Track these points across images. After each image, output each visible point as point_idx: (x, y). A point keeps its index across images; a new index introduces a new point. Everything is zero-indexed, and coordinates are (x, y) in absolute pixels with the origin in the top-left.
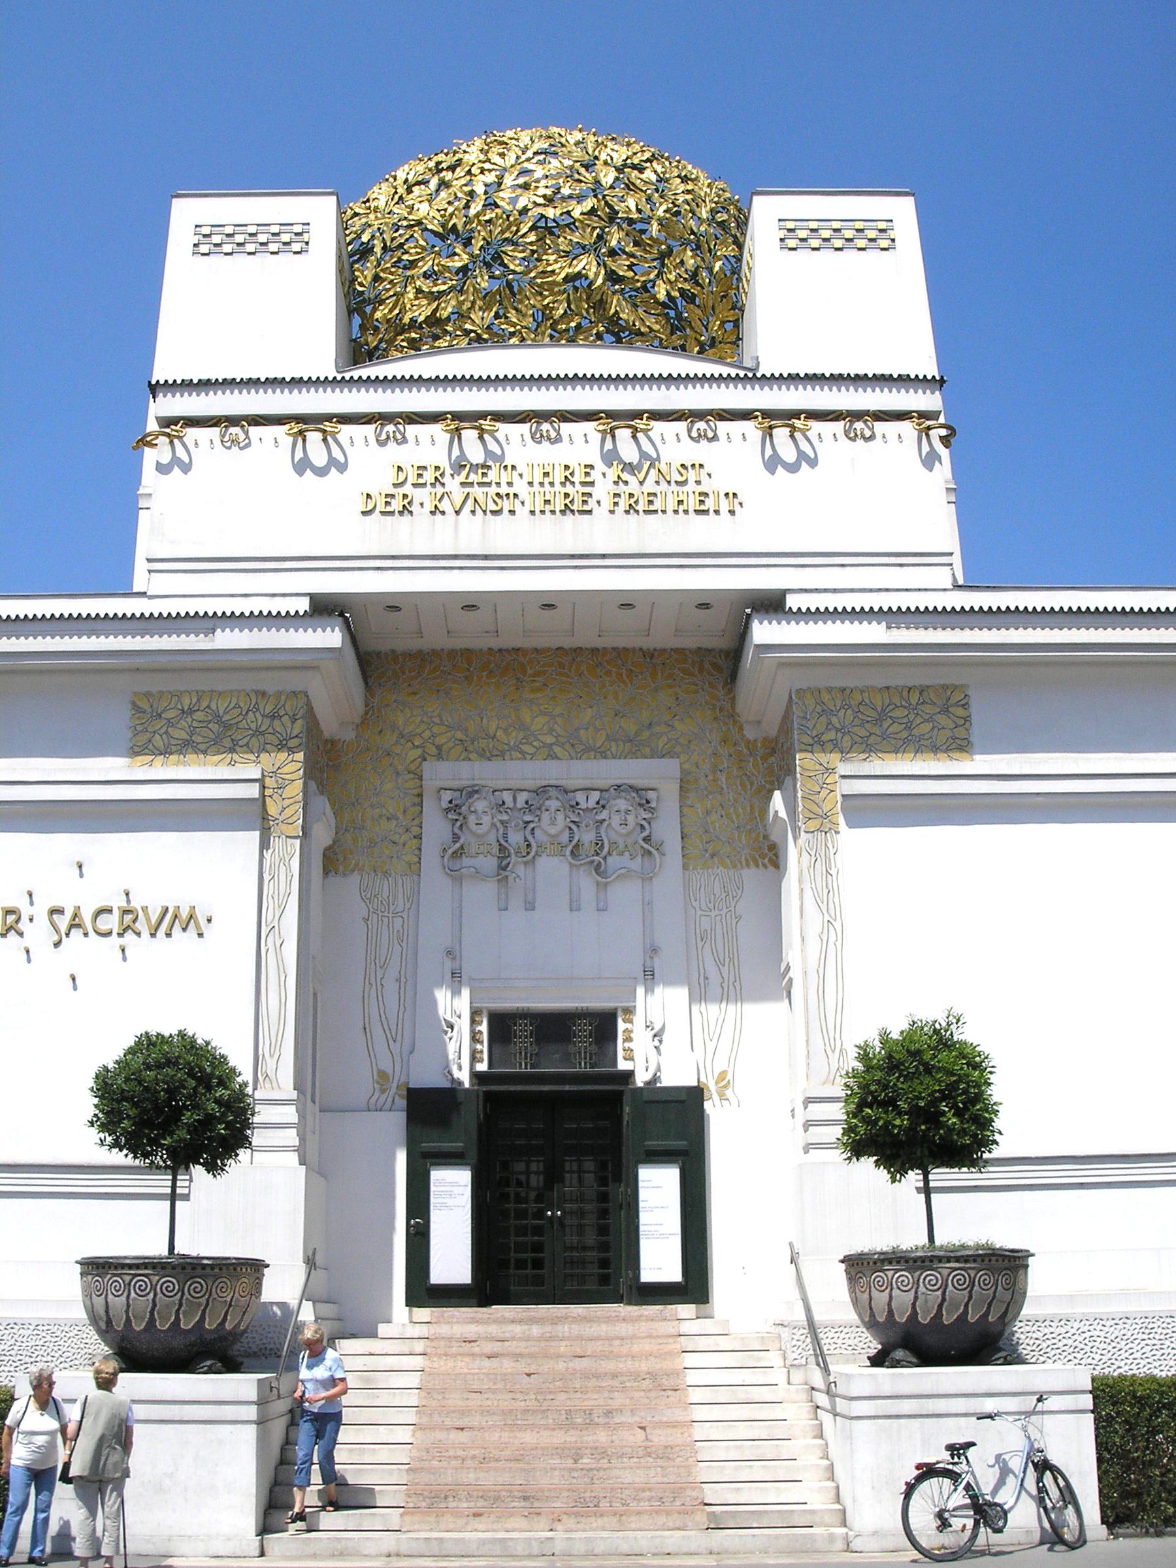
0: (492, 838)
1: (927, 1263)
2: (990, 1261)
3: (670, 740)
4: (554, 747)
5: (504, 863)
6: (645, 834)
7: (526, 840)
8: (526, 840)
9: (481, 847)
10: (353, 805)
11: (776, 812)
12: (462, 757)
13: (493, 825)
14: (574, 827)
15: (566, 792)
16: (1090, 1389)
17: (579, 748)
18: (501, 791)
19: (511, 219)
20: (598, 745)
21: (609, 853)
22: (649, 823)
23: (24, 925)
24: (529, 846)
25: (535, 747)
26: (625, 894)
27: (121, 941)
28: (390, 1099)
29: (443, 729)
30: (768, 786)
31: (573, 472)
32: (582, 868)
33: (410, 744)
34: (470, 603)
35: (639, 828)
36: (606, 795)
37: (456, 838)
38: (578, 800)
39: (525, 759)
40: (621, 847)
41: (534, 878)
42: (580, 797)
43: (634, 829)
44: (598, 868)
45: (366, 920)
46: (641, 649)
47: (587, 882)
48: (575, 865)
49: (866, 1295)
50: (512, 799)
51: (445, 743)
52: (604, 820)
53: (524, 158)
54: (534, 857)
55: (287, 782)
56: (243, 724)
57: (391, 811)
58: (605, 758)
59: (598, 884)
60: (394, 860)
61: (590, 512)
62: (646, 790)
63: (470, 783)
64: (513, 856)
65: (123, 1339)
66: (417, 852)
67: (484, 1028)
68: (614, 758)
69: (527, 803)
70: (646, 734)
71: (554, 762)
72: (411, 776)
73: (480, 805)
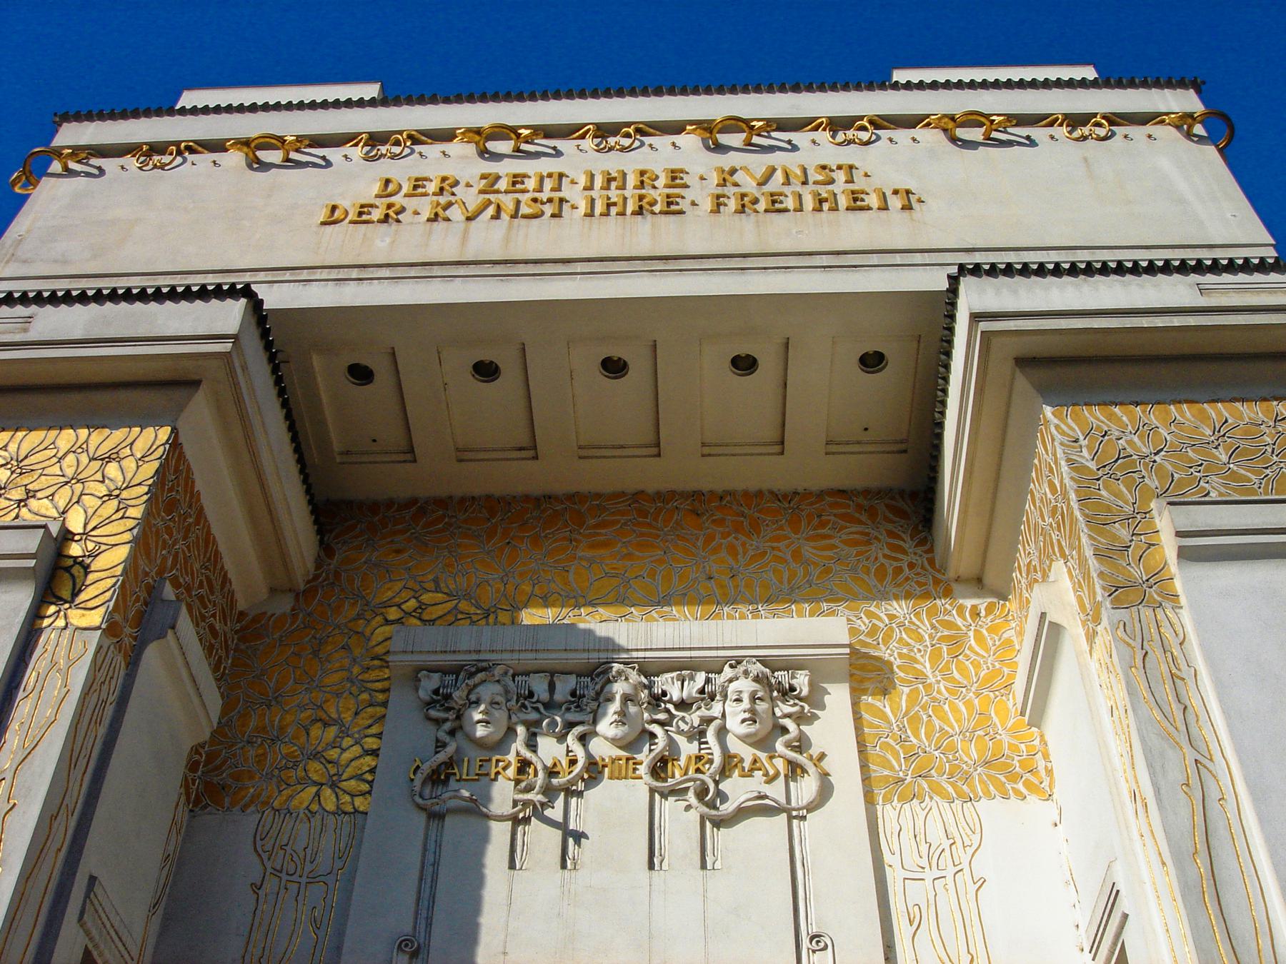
10: (269, 706)
14: (656, 729)
18: (527, 674)
21: (724, 772)
33: (379, 619)
38: (664, 687)
45: (256, 888)
46: (771, 492)
50: (546, 687)
52: (716, 718)
55: (103, 547)
56: (56, 470)
61: (681, 212)
62: (792, 666)
63: (475, 657)
66: (369, 778)
69: (573, 694)
72: (376, 662)
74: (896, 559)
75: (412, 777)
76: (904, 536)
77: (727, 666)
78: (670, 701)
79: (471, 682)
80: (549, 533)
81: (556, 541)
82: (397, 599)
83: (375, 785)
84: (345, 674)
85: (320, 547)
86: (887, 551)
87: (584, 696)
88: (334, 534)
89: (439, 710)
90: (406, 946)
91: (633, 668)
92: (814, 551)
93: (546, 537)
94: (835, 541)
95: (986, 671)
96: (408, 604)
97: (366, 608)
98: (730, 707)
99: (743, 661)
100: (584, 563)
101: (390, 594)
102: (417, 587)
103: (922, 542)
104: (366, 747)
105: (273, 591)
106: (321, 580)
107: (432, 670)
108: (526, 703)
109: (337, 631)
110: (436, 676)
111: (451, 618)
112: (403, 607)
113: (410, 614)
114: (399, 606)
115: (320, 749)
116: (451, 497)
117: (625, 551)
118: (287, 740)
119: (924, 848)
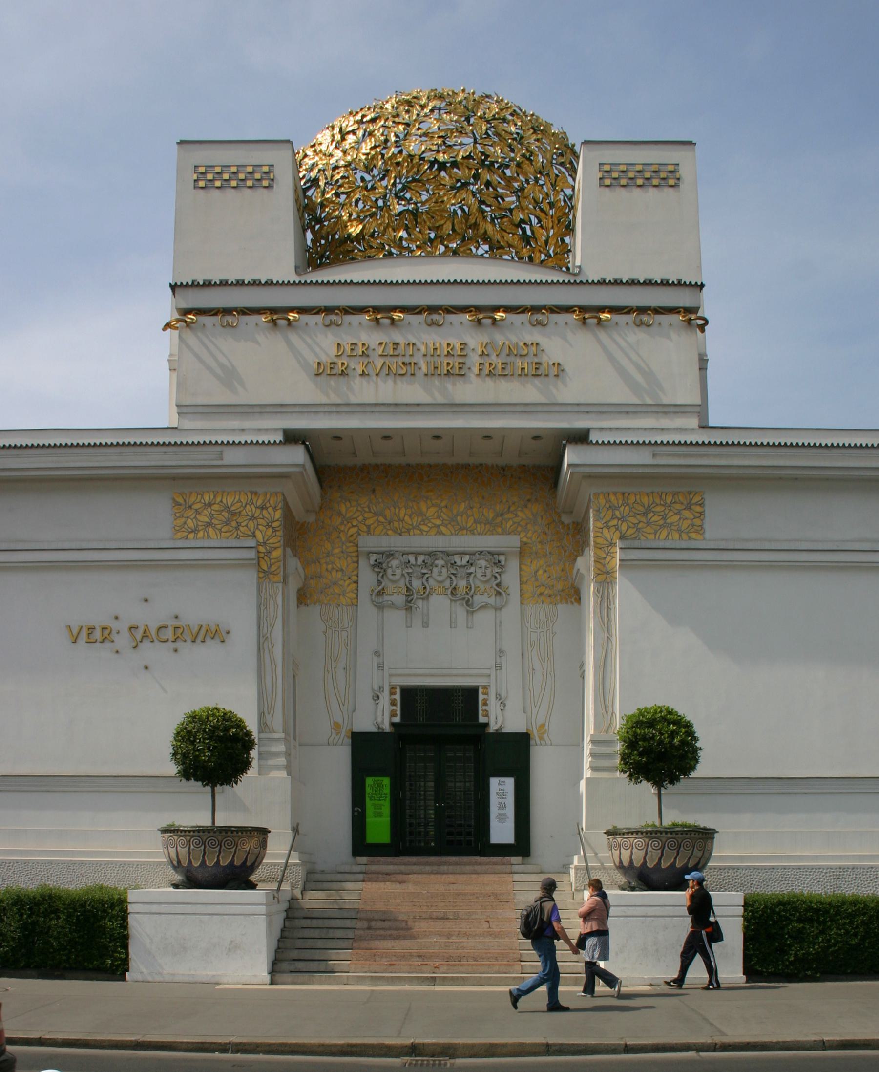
0: (402, 584)
1: (654, 835)
2: (691, 834)
3: (514, 523)
4: (441, 527)
5: (409, 599)
6: (498, 581)
7: (423, 584)
8: (423, 584)
9: (395, 589)
11: (579, 570)
12: (383, 533)
13: (403, 575)
14: (453, 577)
15: (448, 555)
16: (743, 904)
17: (457, 527)
18: (408, 554)
19: (414, 162)
20: (468, 526)
22: (500, 575)
23: (114, 636)
24: (425, 588)
25: (429, 527)
26: (484, 618)
27: (174, 645)
29: (371, 515)
30: (575, 553)
31: (453, 346)
32: (458, 603)
33: (350, 525)
34: (387, 436)
37: (379, 583)
39: (422, 534)
40: (483, 590)
41: (428, 610)
42: (457, 559)
43: (490, 579)
46: (497, 466)
47: (460, 611)
48: (454, 600)
49: (618, 851)
50: (414, 558)
51: (372, 524)
52: (472, 573)
53: (422, 114)
54: (428, 595)
57: (338, 565)
58: (473, 534)
59: (468, 611)
60: (341, 597)
62: (499, 554)
63: (388, 549)
64: (415, 595)
65: (188, 871)
66: (356, 592)
68: (479, 534)
69: (424, 561)
70: (500, 519)
71: (441, 536)
72: (351, 544)
73: (395, 563)
79: (388, 560)
98: (479, 570)
100: (425, 499)
101: (351, 514)
107: (375, 553)
111: (376, 525)
114: (356, 519)
117: (439, 493)
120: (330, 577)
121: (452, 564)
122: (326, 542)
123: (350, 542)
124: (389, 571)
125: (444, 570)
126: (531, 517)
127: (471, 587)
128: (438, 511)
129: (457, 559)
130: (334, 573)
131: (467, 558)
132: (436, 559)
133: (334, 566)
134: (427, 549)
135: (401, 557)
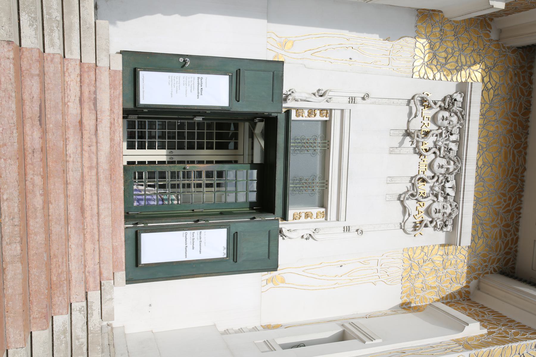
10: (454, 36)
28: (273, 48)
32: (410, 184)
33: (485, 74)
35: (430, 219)
36: (452, 200)
44: (412, 195)
46: (520, 217)
50: (455, 139)
52: (438, 199)
62: (454, 225)
66: (425, 77)
67: (318, 117)
69: (451, 149)
73: (455, 119)
74: (489, 262)
75: (425, 93)
76: (498, 264)
77: (456, 204)
78: (445, 182)
80: (513, 136)
81: (509, 139)
82: (492, 80)
83: (423, 80)
84: (464, 63)
85: (517, 47)
86: (493, 258)
87: (449, 154)
88: (522, 52)
89: (449, 101)
90: (367, 96)
91: (458, 171)
92: (495, 232)
93: (511, 135)
94: (498, 240)
95: (445, 289)
96: (490, 85)
97: (490, 69)
99: (458, 209)
100: (499, 150)
102: (496, 88)
103: (495, 271)
104: (436, 75)
105: (500, 31)
106: (503, 49)
108: (449, 133)
109: (481, 58)
110: (461, 99)
112: (489, 83)
113: (486, 86)
114: (489, 81)
115: (437, 57)
116: (532, 97)
118: (441, 44)
119: (388, 267)
120: (440, 50)
121: (448, 177)
122: (472, 49)
123: (469, 73)
124: (446, 114)
125: (443, 171)
126: (477, 252)
127: (425, 198)
128: (489, 163)
129: (452, 183)
130: (444, 55)
131: (452, 193)
132: (455, 163)
133: (450, 56)
134: (465, 154)
135: (458, 125)
